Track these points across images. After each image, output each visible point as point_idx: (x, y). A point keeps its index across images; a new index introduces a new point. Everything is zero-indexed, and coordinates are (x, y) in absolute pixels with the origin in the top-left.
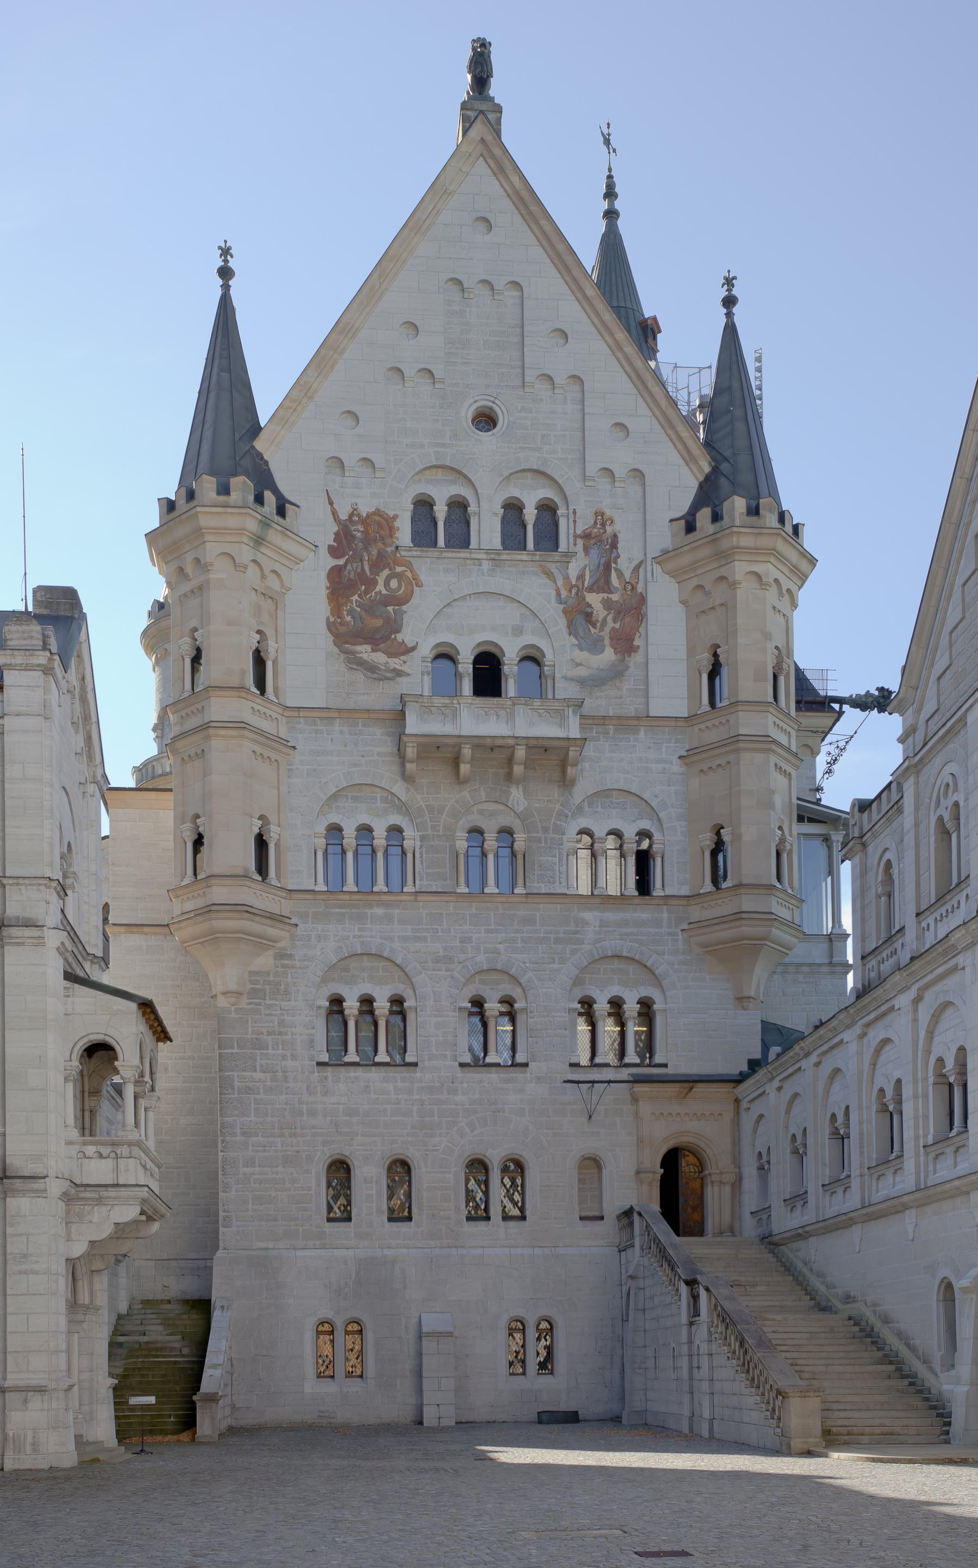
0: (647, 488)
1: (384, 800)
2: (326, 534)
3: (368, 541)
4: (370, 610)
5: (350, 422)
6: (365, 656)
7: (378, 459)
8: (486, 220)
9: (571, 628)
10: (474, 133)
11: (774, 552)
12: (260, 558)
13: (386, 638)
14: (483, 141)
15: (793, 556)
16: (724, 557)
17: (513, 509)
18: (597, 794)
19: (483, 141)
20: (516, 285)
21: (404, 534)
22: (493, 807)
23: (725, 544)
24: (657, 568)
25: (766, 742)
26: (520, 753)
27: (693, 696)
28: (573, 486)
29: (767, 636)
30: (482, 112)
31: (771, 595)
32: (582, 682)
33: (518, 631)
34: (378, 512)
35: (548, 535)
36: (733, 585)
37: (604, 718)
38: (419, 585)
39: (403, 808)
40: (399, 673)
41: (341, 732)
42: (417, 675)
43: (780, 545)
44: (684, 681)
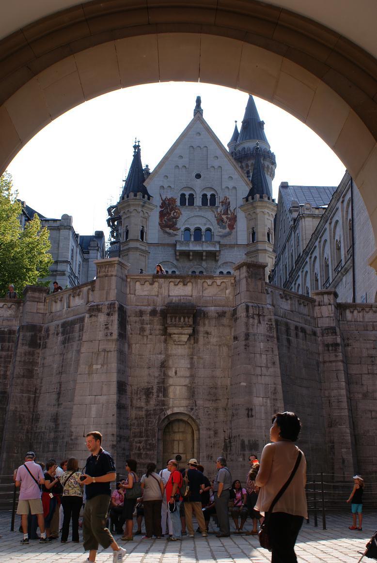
0: (237, 191)
1: (171, 265)
2: (159, 203)
3: (169, 204)
5: (166, 178)
6: (168, 231)
7: (173, 186)
8: (199, 133)
9: (218, 224)
10: (197, 116)
11: (266, 206)
12: (143, 210)
13: (173, 226)
14: (199, 117)
15: (272, 207)
16: (255, 208)
17: (205, 196)
18: (224, 263)
19: (199, 117)
20: (206, 147)
21: (178, 203)
24: (239, 209)
25: (265, 250)
26: (204, 254)
27: (248, 239)
29: (266, 226)
30: (198, 111)
31: (267, 216)
32: (221, 236)
33: (205, 224)
34: (172, 198)
35: (213, 202)
36: (257, 214)
37: (226, 245)
38: (181, 214)
39: (176, 267)
40: (176, 235)
41: (161, 249)
42: (180, 236)
43: (268, 205)
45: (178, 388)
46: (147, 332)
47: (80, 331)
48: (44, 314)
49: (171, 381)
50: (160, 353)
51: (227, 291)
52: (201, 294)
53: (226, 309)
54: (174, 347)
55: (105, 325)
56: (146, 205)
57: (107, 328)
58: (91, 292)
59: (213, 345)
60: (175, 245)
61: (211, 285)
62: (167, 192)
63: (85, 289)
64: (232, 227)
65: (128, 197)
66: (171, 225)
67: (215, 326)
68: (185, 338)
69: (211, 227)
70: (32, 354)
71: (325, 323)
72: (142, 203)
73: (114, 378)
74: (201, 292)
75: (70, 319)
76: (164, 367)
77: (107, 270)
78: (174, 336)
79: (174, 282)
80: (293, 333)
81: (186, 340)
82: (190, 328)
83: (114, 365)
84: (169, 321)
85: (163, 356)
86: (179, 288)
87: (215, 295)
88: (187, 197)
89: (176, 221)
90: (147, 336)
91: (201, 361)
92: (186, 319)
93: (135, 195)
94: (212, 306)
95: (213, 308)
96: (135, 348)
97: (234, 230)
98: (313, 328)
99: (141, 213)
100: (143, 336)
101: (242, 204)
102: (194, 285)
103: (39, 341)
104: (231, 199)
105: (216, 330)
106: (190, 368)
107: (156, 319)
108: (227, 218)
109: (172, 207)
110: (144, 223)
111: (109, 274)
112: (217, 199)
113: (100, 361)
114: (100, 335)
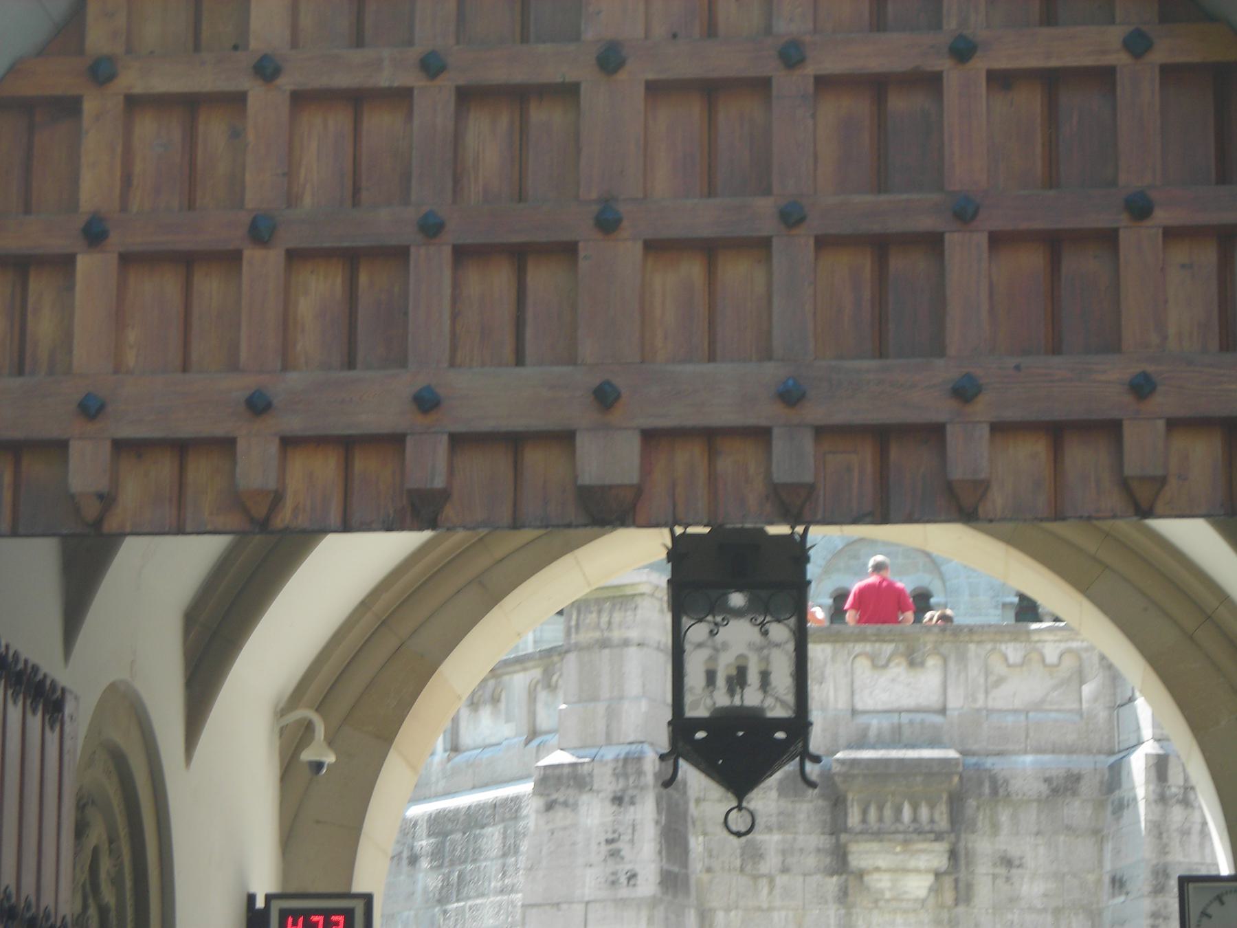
46: (771, 863)
47: (504, 855)
51: (1087, 690)
52: (980, 703)
53: (1082, 763)
55: (608, 842)
57: (615, 854)
58: (543, 695)
59: (1031, 909)
61: (1022, 665)
63: (519, 681)
67: (1037, 834)
68: (918, 886)
77: (605, 619)
81: (922, 893)
84: (854, 819)
86: (893, 680)
87: (1038, 706)
90: (771, 880)
94: (1026, 752)
95: (1029, 758)
100: (756, 878)
102: (952, 664)
105: (1042, 850)
111: (616, 635)
114: (590, 882)
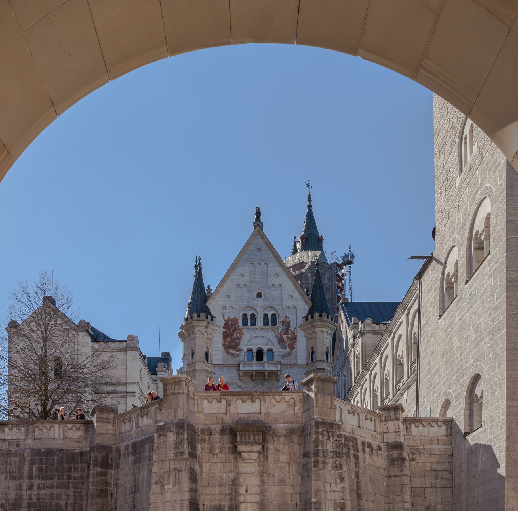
1: (236, 385)
2: (222, 324)
3: (232, 325)
4: (232, 341)
9: (279, 344)
12: (207, 331)
13: (236, 347)
15: (331, 326)
22: (260, 386)
23: (314, 324)
28: (280, 310)
31: (326, 335)
33: (267, 345)
34: (234, 318)
35: (274, 322)
36: (316, 333)
38: (244, 335)
40: (239, 356)
43: (327, 323)
44: (306, 355)
45: (249, 505)
46: (217, 451)
47: (150, 451)
48: (114, 435)
49: (242, 499)
50: (231, 472)
54: (244, 464)
56: (210, 326)
59: (282, 462)
60: (239, 366)
62: (230, 312)
64: (292, 347)
65: (192, 317)
66: (234, 346)
68: (255, 456)
69: (273, 348)
70: (104, 474)
71: (391, 438)
72: (205, 324)
73: (187, 496)
74: (270, 409)
75: (140, 439)
76: (235, 485)
78: (244, 454)
79: (242, 400)
80: (360, 448)
81: (256, 458)
82: (259, 446)
83: (186, 485)
84: (238, 439)
85: (233, 475)
87: (284, 412)
88: (249, 317)
89: (239, 342)
90: (217, 455)
91: (271, 478)
92: (256, 437)
93: (199, 316)
95: (282, 425)
96: (206, 467)
97: (295, 350)
98: (380, 444)
99: (205, 334)
100: (213, 455)
101: (302, 323)
103: (110, 462)
104: (292, 319)
106: (261, 485)
107: (227, 437)
108: (288, 338)
109: (235, 328)
110: (208, 344)
112: (277, 318)
113: (171, 481)
